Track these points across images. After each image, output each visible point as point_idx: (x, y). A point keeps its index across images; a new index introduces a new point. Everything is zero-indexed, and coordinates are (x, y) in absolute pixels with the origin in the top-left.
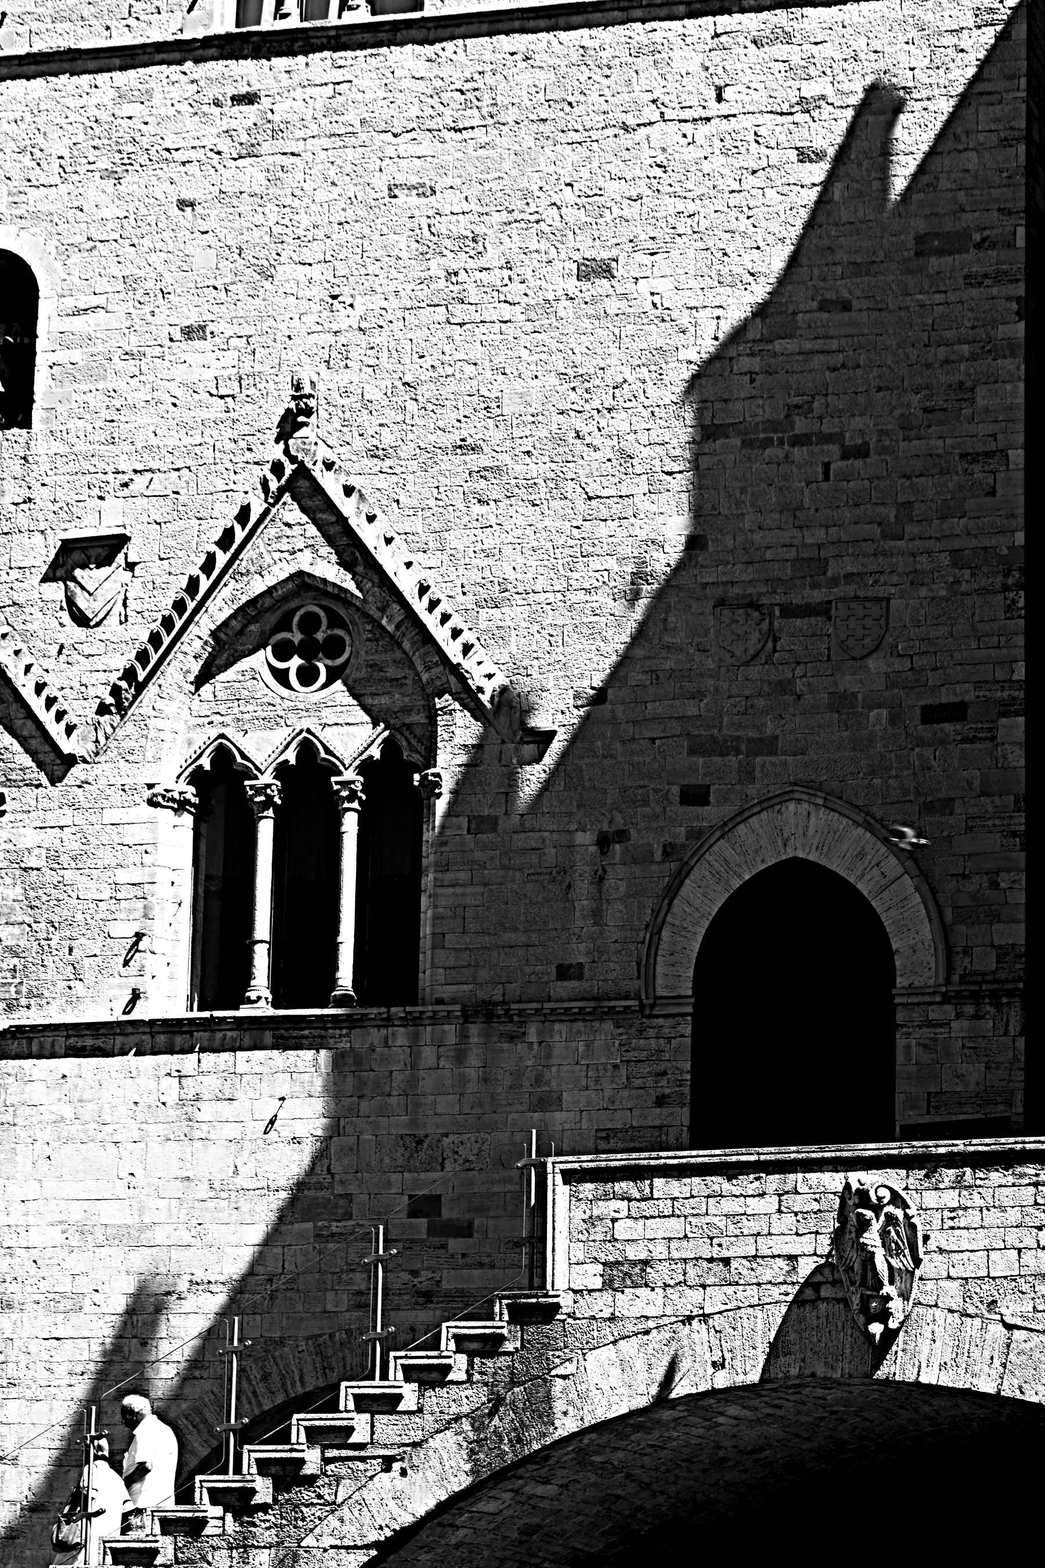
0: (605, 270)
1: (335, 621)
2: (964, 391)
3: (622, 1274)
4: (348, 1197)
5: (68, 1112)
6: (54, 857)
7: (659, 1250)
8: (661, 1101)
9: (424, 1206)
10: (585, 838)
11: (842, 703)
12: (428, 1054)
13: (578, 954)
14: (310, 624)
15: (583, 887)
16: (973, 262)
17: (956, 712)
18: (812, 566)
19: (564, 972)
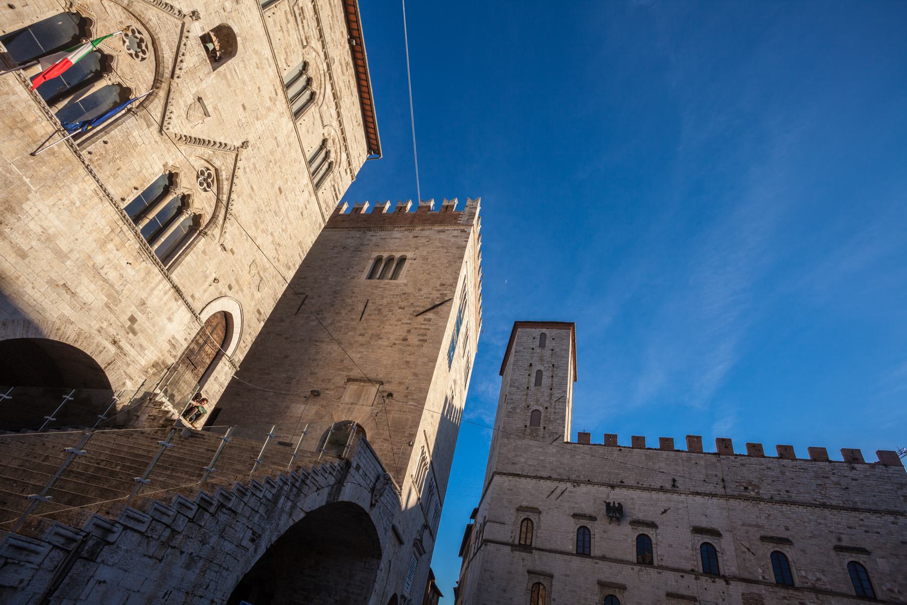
0: (281, 192)
1: (213, 181)
4: (120, 301)
5: (78, 204)
6: (136, 145)
9: (133, 319)
10: (214, 276)
12: (161, 287)
13: (197, 295)
15: (207, 284)
19: (192, 296)
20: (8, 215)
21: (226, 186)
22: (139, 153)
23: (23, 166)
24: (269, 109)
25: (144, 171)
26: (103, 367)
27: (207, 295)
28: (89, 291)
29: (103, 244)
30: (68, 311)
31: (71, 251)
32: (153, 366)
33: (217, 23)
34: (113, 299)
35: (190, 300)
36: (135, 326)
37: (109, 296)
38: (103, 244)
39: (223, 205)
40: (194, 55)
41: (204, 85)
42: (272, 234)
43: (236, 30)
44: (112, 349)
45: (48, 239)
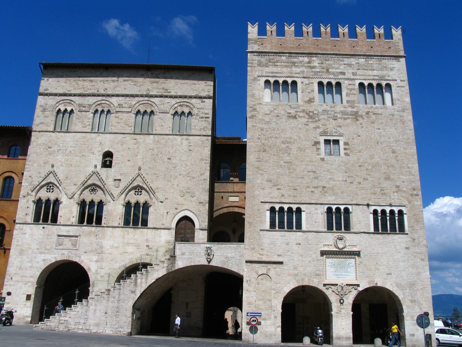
2: (204, 174)
3: (183, 254)
5: (111, 235)
7: (187, 252)
8: (172, 237)
9: (148, 246)
10: (166, 212)
11: (191, 201)
13: (164, 223)
14: (139, 189)
15: (165, 217)
16: (205, 161)
17: (202, 203)
18: (189, 188)
19: (163, 224)
20: (102, 249)
21: (145, 186)
22: (114, 211)
23: (97, 239)
24: (138, 147)
25: (118, 212)
26: (149, 262)
27: (168, 220)
28: (130, 249)
29: (124, 237)
30: (130, 257)
31: (119, 245)
32: (166, 252)
33: (101, 157)
34: (138, 246)
35: (162, 227)
36: (150, 247)
37: (136, 246)
38: (124, 237)
39: (150, 191)
40: (104, 172)
41: (112, 175)
42: (180, 175)
43: (106, 150)
44: (148, 257)
45: (112, 247)
